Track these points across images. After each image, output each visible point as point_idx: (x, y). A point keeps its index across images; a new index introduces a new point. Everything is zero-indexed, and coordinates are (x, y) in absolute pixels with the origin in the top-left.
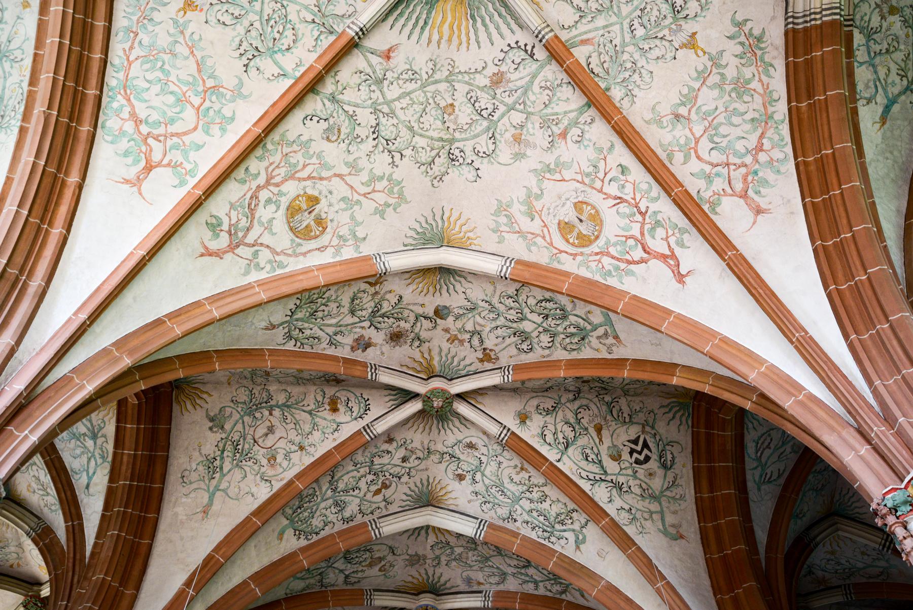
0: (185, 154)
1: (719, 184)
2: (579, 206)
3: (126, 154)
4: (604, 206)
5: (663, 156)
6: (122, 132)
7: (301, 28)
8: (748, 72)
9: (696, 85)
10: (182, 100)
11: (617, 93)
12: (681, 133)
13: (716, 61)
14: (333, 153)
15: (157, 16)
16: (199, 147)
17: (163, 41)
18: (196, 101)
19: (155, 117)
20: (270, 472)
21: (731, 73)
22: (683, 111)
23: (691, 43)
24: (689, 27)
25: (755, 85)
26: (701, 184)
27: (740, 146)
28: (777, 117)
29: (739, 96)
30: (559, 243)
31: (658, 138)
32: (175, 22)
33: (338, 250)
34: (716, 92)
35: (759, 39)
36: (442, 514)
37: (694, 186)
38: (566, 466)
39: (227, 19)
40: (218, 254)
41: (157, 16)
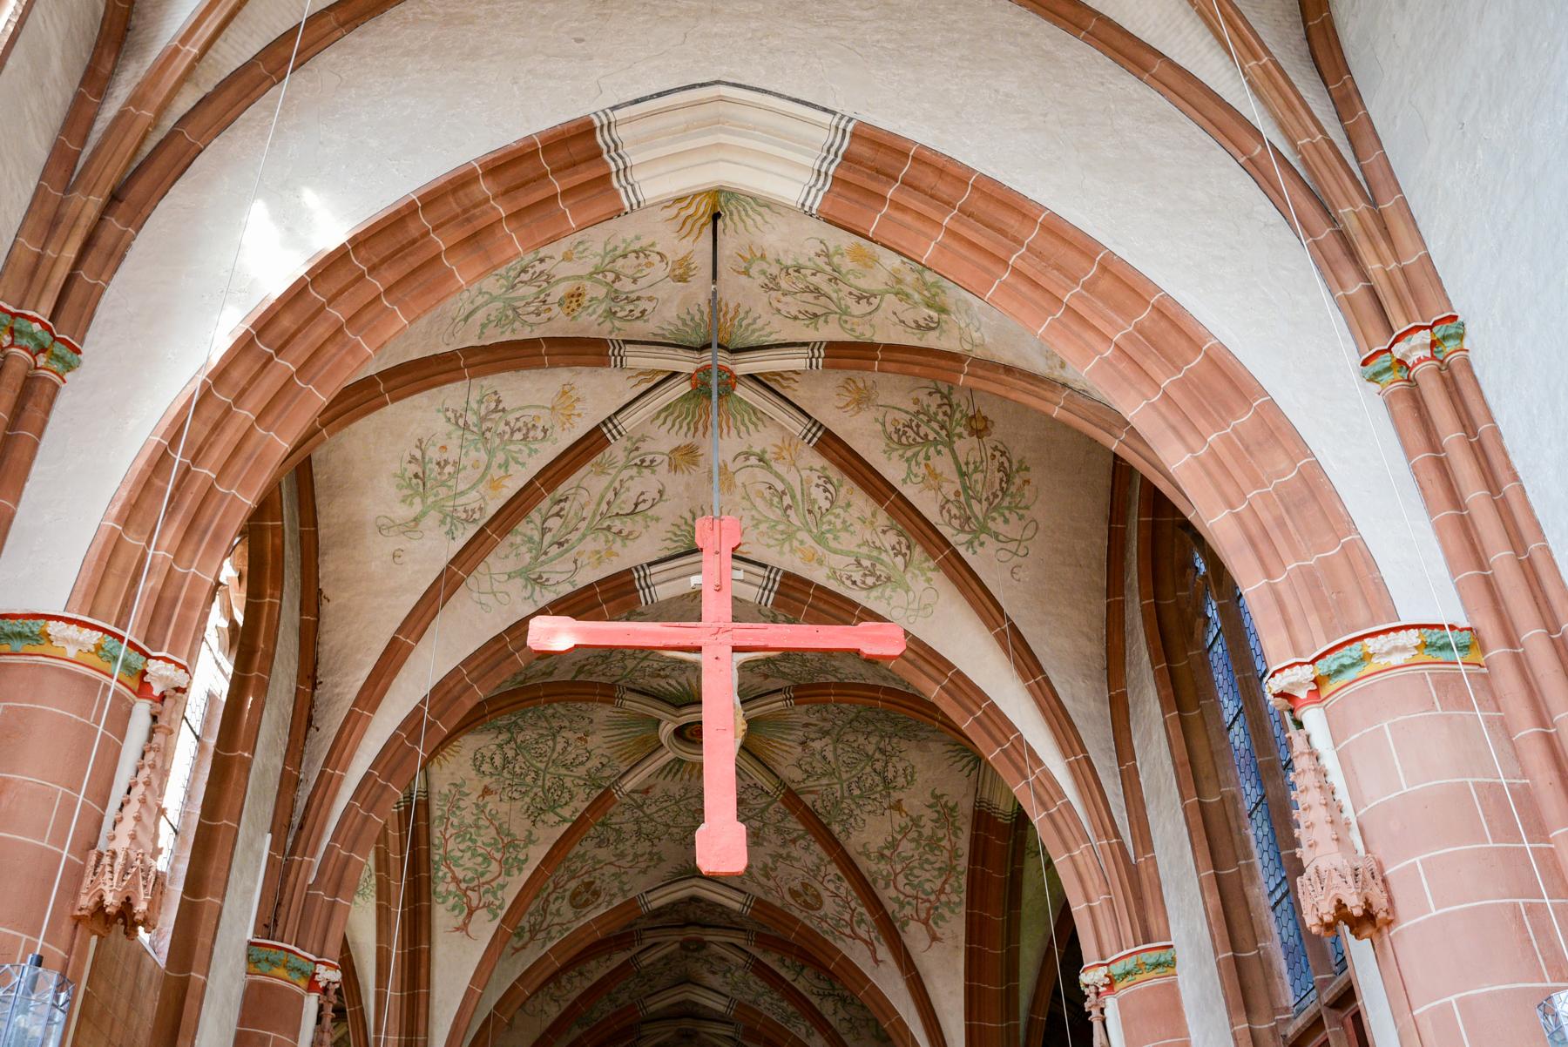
0: (495, 895)
1: (908, 910)
2: (804, 885)
3: (453, 909)
4: (825, 894)
5: (869, 880)
6: (449, 893)
7: (575, 790)
8: (940, 833)
9: (899, 837)
10: (487, 859)
11: (836, 828)
12: (884, 867)
13: (916, 822)
14: (603, 854)
15: (462, 804)
16: (503, 887)
17: (469, 820)
18: (498, 856)
19: (470, 875)
20: (557, 993)
21: (927, 832)
22: (887, 852)
23: (897, 807)
24: (896, 795)
25: (944, 843)
26: (896, 906)
27: (927, 886)
28: (960, 869)
29: (932, 850)
30: (788, 897)
31: (867, 866)
32: (477, 805)
33: (610, 903)
34: (913, 845)
35: (953, 809)
36: (699, 991)
37: (891, 907)
38: (801, 985)
39: (516, 795)
40: (524, 947)
41: (462, 804)
